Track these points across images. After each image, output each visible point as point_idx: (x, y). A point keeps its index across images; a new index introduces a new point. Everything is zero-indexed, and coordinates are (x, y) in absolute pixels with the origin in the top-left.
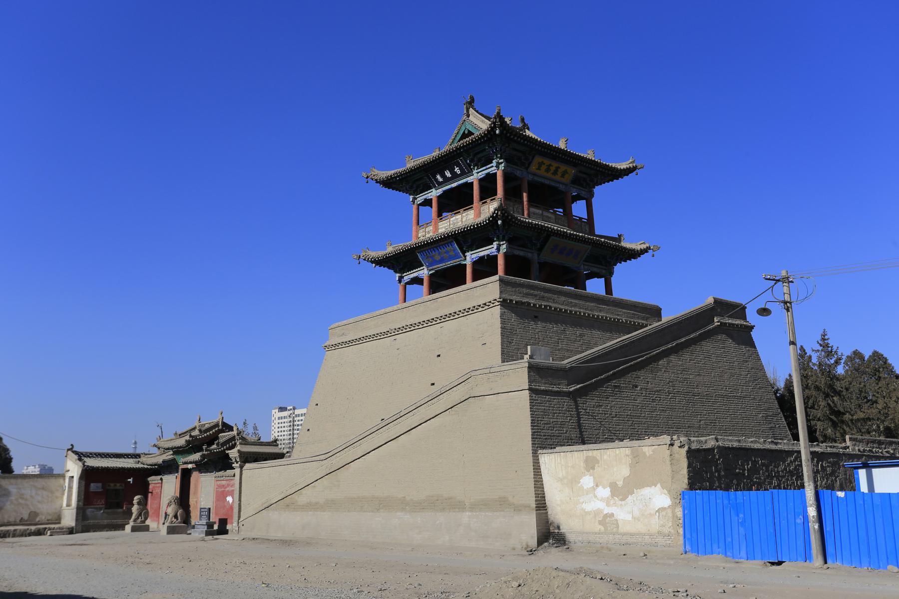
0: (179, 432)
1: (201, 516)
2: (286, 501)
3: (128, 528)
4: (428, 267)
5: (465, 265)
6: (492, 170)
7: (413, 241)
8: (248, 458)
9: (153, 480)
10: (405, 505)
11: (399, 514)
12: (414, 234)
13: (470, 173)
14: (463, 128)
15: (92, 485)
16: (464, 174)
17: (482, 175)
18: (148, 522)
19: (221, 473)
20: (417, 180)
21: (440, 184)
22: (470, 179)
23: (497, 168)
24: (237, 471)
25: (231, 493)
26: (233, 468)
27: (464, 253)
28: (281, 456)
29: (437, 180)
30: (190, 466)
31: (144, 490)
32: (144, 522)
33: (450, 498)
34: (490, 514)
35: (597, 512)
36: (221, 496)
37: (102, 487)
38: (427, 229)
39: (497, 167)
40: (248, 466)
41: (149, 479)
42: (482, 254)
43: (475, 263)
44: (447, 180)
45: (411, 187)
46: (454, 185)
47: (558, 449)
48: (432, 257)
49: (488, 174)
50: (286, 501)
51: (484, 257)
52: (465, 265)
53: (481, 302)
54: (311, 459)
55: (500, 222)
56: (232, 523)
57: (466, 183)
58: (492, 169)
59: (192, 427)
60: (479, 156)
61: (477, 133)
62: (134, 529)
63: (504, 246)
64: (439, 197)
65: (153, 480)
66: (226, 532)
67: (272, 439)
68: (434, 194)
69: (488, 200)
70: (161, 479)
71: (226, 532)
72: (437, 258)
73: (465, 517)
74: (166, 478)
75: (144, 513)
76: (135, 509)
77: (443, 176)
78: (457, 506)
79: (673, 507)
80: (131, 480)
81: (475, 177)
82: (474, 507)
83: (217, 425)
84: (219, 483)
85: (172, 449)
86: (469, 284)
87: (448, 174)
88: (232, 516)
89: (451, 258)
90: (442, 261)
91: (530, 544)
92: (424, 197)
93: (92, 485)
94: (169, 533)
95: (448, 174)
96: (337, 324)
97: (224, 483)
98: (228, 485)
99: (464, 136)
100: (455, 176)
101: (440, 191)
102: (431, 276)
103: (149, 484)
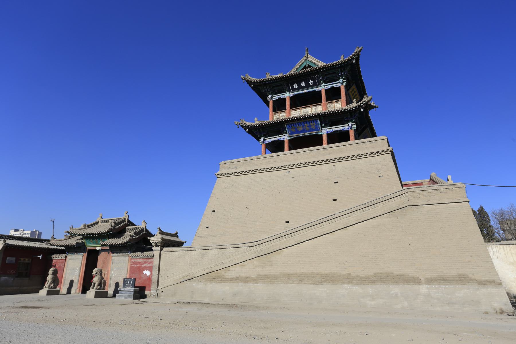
0: (88, 224)
1: (124, 285)
2: (213, 276)
3: (43, 292)
4: (290, 134)
5: (322, 135)
6: (336, 85)
7: (270, 120)
8: (166, 244)
9: (55, 257)
10: (349, 279)
11: (345, 286)
12: (270, 116)
13: (319, 85)
14: (305, 64)
15: (8, 258)
16: (315, 85)
17: (329, 86)
18: (58, 288)
19: (139, 253)
20: (273, 87)
21: (294, 90)
22: (318, 89)
23: (341, 84)
24: (156, 253)
25: (150, 269)
26: (152, 250)
27: (322, 127)
28: (180, 244)
29: (293, 87)
30: (99, 248)
31: (48, 263)
32: (55, 287)
33: (401, 275)
34: (450, 287)
36: (136, 269)
37: (16, 260)
38: (281, 115)
39: (342, 83)
40: (165, 249)
41: (53, 256)
42: (336, 129)
43: (329, 135)
44: (300, 88)
45: (271, 90)
46: (304, 91)
47: (503, 242)
48: (296, 129)
49: (332, 88)
50: (213, 276)
51: (337, 131)
52: (322, 135)
53: (374, 151)
54: (238, 246)
55: (362, 110)
56: (150, 290)
57: (315, 91)
58: (336, 85)
59: (96, 221)
60: (328, 76)
61: (315, 67)
62: (49, 293)
63: (355, 126)
64: (291, 98)
65: (55, 257)
66: (145, 297)
67: (174, 233)
68: (287, 95)
69: (334, 101)
70: (66, 257)
71: (145, 297)
72: (300, 129)
73: (424, 289)
74: (70, 256)
75: (56, 281)
76: (49, 278)
80: (40, 256)
81: (323, 88)
82: (430, 281)
83: (124, 221)
84: (133, 261)
86: (325, 145)
88: (150, 286)
90: (304, 131)
91: (505, 308)
92: (279, 97)
93: (8, 258)
94: (95, 297)
95: (303, 84)
96: (227, 161)
98: (145, 263)
99: (305, 67)
100: (308, 86)
101: (292, 94)
102: (290, 141)
103: (52, 260)
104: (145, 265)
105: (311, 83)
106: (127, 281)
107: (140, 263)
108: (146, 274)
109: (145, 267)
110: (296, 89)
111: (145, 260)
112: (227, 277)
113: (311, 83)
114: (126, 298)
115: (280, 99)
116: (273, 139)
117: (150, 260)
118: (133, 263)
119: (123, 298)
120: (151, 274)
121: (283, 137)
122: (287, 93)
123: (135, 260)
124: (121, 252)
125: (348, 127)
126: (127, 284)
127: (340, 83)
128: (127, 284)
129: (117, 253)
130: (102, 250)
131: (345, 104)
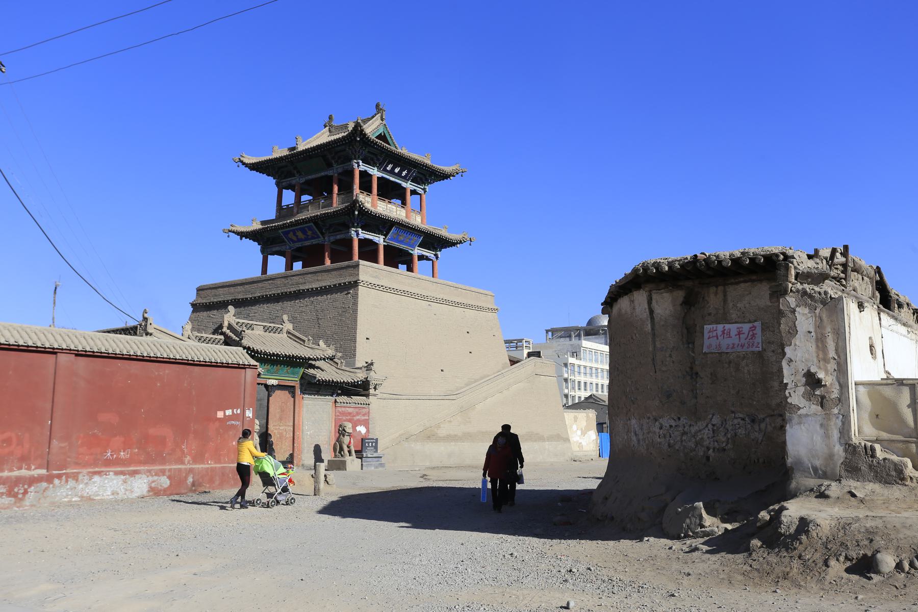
16: (405, 179)
21: (385, 170)
22: (404, 184)
25: (366, 423)
26: (367, 396)
44: (391, 172)
46: (392, 179)
72: (402, 238)
77: (393, 169)
84: (340, 409)
87: (397, 170)
89: (406, 244)
90: (401, 242)
97: (350, 410)
98: (358, 414)
100: (399, 175)
104: (358, 417)
105: (404, 173)
107: (350, 414)
110: (387, 171)
111: (357, 410)
112: (441, 435)
113: (404, 173)
114: (376, 467)
115: (366, 171)
117: (364, 411)
120: (368, 431)
122: (376, 169)
124: (318, 393)
127: (424, 189)
129: (311, 394)
130: (280, 387)
131: (425, 221)
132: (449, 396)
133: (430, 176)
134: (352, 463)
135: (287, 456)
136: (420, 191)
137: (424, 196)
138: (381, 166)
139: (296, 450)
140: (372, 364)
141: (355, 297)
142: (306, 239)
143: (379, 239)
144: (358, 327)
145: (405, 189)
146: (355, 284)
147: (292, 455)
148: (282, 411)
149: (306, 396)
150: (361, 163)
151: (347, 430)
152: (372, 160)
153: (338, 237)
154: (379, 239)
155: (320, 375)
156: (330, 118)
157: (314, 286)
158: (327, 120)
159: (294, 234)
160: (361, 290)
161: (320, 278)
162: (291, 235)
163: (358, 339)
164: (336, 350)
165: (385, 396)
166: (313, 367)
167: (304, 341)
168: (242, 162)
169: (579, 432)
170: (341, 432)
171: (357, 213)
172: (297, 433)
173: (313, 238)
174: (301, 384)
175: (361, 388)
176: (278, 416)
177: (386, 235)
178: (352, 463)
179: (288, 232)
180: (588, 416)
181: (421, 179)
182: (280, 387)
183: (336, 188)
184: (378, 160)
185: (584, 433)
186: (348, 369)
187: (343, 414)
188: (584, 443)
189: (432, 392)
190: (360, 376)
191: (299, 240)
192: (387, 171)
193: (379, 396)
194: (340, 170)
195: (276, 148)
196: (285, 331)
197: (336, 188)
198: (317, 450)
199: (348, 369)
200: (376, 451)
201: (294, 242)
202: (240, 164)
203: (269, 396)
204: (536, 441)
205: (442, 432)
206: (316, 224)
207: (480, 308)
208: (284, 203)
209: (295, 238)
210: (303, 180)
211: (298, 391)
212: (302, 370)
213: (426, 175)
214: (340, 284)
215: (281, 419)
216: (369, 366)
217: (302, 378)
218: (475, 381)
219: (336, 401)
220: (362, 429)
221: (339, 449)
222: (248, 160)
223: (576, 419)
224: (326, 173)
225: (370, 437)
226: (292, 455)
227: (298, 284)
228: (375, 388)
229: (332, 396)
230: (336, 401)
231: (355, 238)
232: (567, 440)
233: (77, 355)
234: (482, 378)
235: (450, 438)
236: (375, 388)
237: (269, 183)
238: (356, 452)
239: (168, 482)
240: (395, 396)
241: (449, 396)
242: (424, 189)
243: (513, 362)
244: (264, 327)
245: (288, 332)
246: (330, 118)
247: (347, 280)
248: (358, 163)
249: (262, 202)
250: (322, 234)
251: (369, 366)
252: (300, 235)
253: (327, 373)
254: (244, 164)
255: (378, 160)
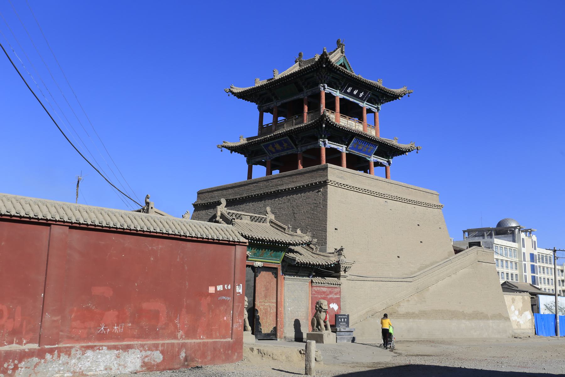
16: (362, 99)
21: (346, 93)
22: (361, 104)
26: (338, 277)
33: (482, 313)
35: (516, 320)
44: (351, 94)
46: (351, 100)
48: (358, 145)
57: (358, 104)
72: (360, 147)
77: (352, 91)
78: (485, 317)
79: (532, 319)
85: (252, 239)
87: (355, 92)
90: (360, 151)
97: (324, 289)
98: (331, 293)
100: (357, 96)
104: (331, 296)
105: (361, 95)
106: (341, 319)
107: (324, 292)
108: (333, 308)
109: (331, 298)
110: (347, 93)
111: (330, 289)
113: (361, 95)
115: (330, 93)
116: (333, 146)
117: (336, 290)
118: (316, 292)
119: (345, 341)
120: (340, 308)
121: (340, 148)
123: (318, 289)
125: (386, 162)
126: (341, 322)
127: (377, 108)
128: (341, 322)
130: (265, 269)
131: (379, 134)
132: (407, 279)
133: (382, 97)
134: (329, 336)
135: (271, 329)
136: (374, 109)
137: (377, 114)
138: (342, 89)
139: (279, 324)
140: (342, 249)
141: (325, 194)
142: (283, 150)
143: (343, 148)
144: (328, 219)
145: (362, 108)
146: (325, 184)
147: (275, 329)
148: (267, 289)
149: (287, 277)
150: (326, 87)
151: (324, 307)
152: (335, 84)
153: (309, 147)
154: (343, 148)
155: (299, 259)
156: (300, 55)
157: (290, 186)
158: (297, 57)
159: (273, 146)
160: (330, 188)
161: (295, 180)
162: (270, 147)
163: (328, 230)
164: (313, 237)
165: (353, 277)
166: (293, 251)
167: (284, 229)
168: (231, 92)
169: (517, 313)
170: (318, 308)
171: (324, 126)
172: (279, 309)
173: (288, 149)
174: (283, 267)
175: (333, 271)
176: (263, 293)
177: (347, 145)
178: (329, 336)
179: (268, 145)
180: (523, 299)
181: (375, 100)
182: (265, 269)
183: (306, 108)
184: (340, 84)
185: (521, 313)
186: (321, 253)
187: (318, 292)
188: (521, 322)
189: (391, 275)
190: (333, 260)
191: (277, 151)
192: (347, 93)
193: (348, 278)
194: (309, 94)
195: (258, 80)
196: (268, 220)
197: (306, 108)
198: (297, 324)
199: (321, 253)
200: (348, 326)
201: (273, 153)
202: (230, 93)
203: (255, 276)
204: (481, 319)
205: (402, 310)
206: (290, 137)
207: (428, 205)
208: (265, 123)
209: (273, 150)
210: (279, 104)
211: (280, 272)
212: (283, 254)
213: (379, 96)
214: (312, 184)
215: (266, 296)
216: (339, 252)
217: (283, 261)
218: (427, 266)
219: (312, 282)
220: (335, 306)
221: (316, 323)
222: (237, 90)
223: (513, 301)
224: (298, 97)
225: (342, 313)
226: (275, 329)
227: (277, 185)
228: (345, 271)
229: (309, 277)
230: (312, 282)
231: (323, 147)
232: (508, 319)
233: (71, 227)
234: (432, 264)
235: (408, 315)
236: (345, 271)
237: (252, 108)
238: (331, 326)
239: (161, 357)
240: (362, 278)
241: (407, 279)
242: (377, 108)
243: (457, 251)
244: (251, 217)
245: (271, 222)
246: (300, 55)
247: (318, 180)
248: (324, 87)
249: (247, 123)
250: (296, 145)
251: (339, 252)
252: (278, 147)
253: (305, 256)
254: (233, 93)
255: (340, 84)
